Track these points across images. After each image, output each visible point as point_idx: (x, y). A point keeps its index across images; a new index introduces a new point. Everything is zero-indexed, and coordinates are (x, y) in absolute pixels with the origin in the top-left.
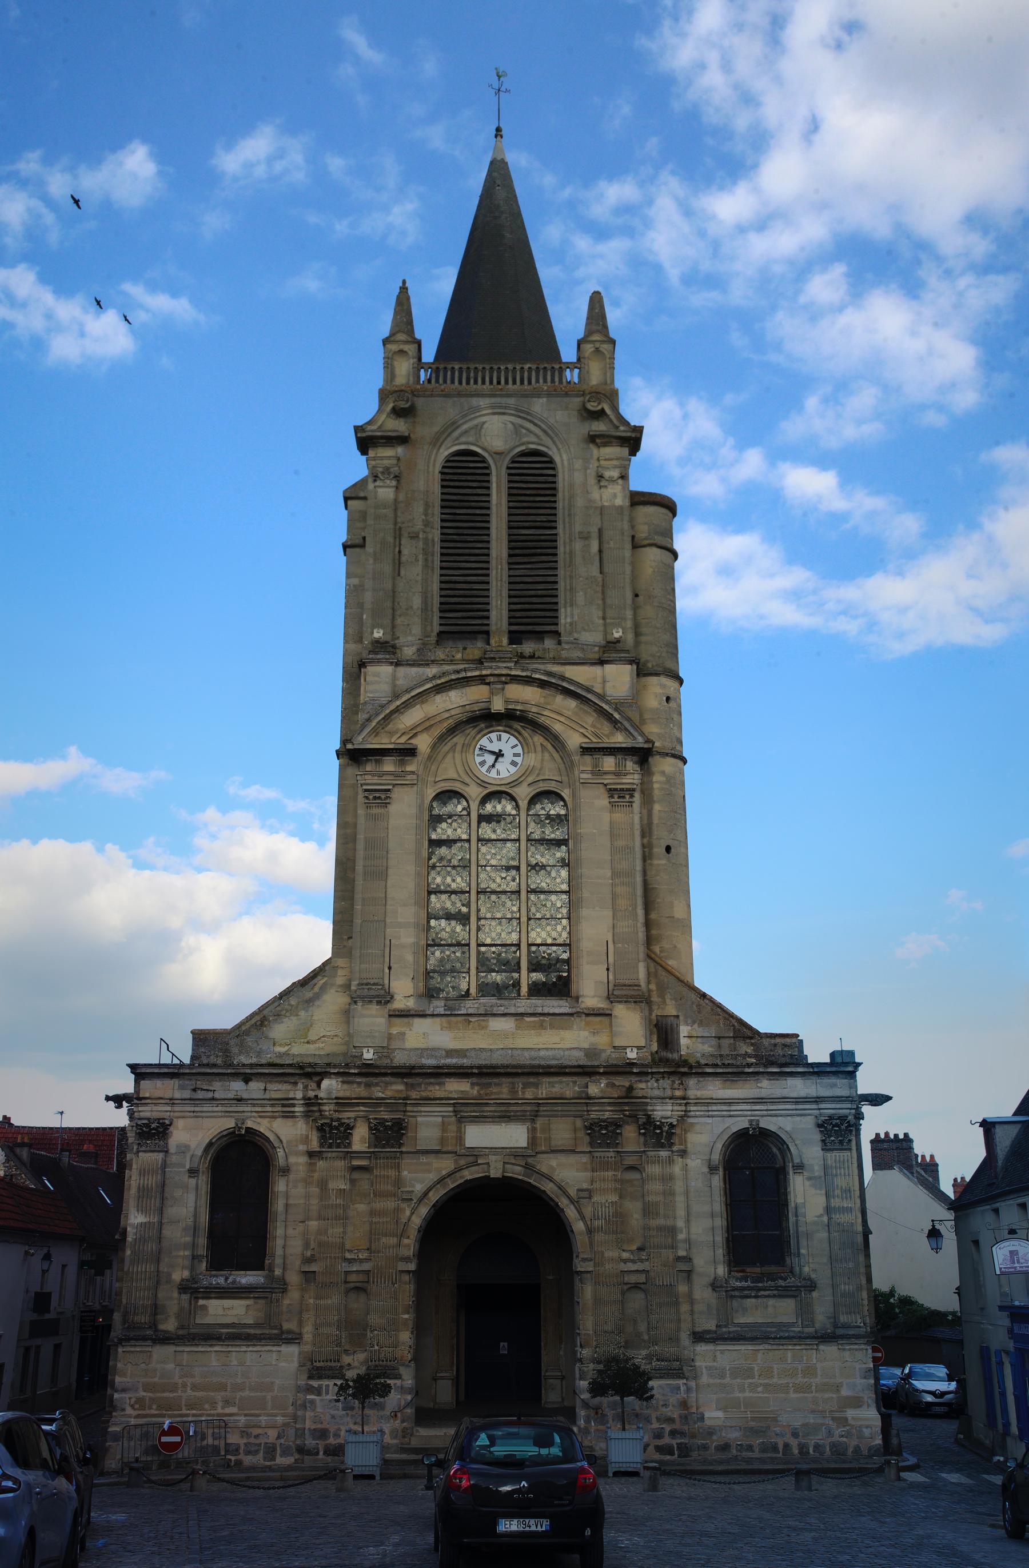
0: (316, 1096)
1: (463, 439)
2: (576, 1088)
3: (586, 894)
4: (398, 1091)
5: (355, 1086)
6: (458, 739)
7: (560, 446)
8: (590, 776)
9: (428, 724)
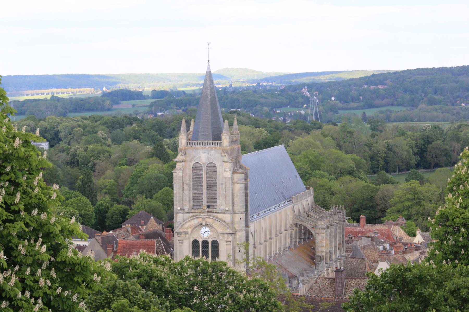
6: (197, 228)
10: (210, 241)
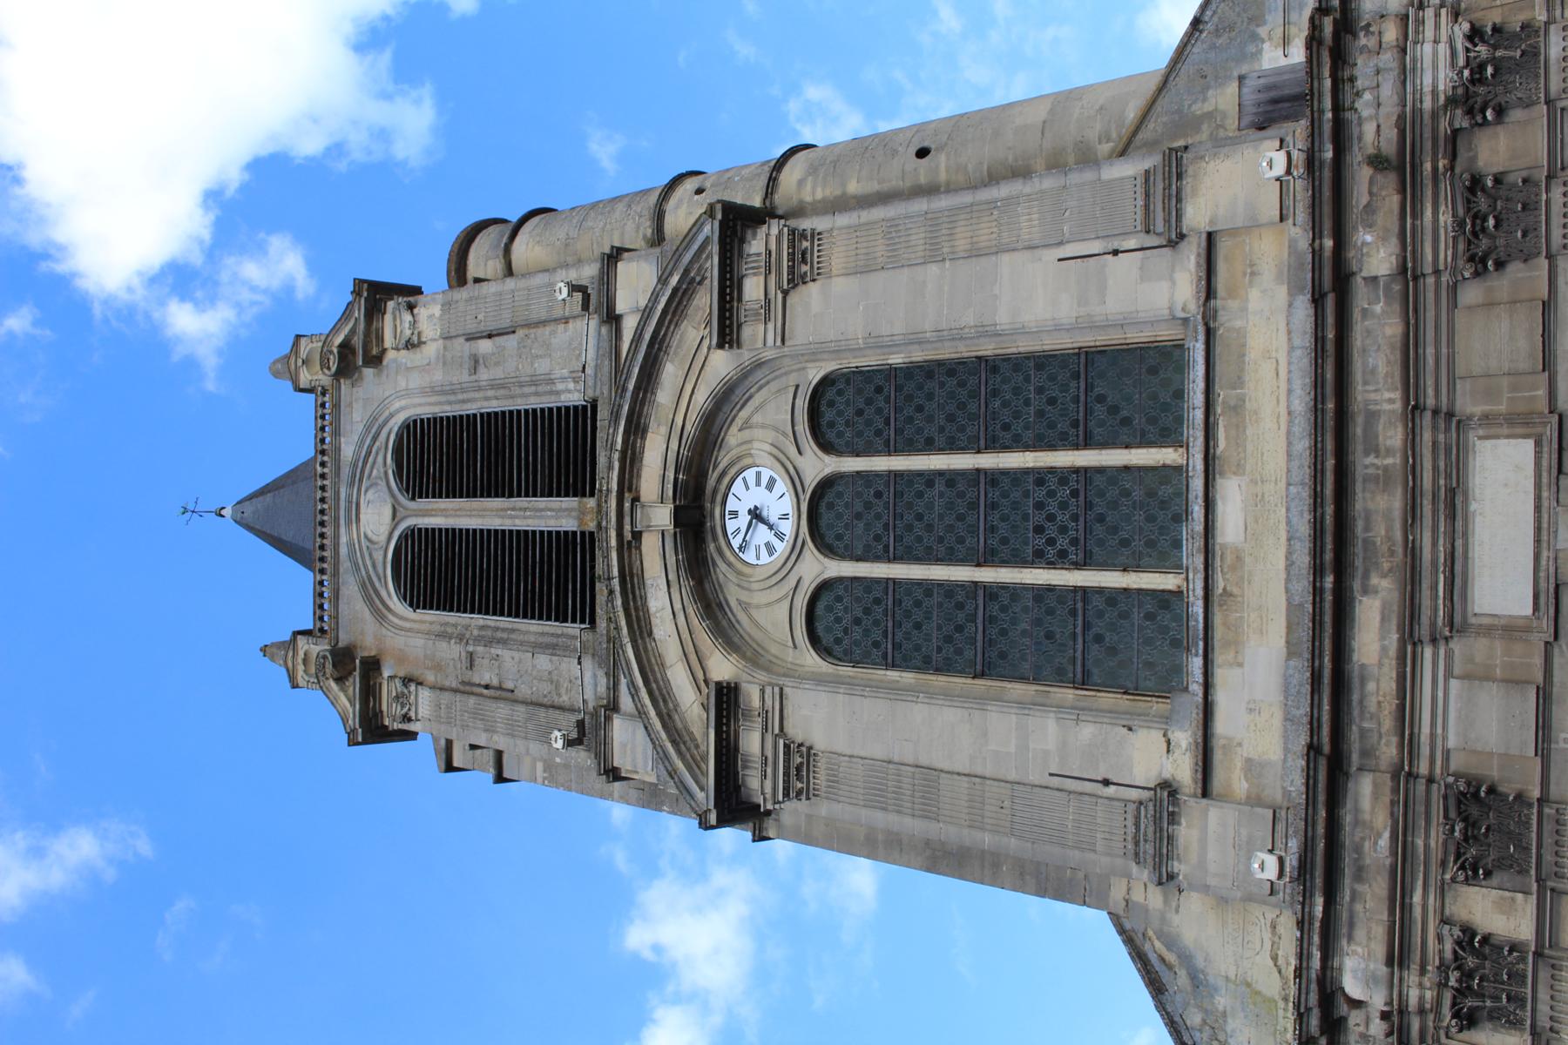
0: (1385, 1016)
1: (380, 571)
2: (1378, 308)
3: (969, 319)
4: (1376, 796)
5: (1359, 907)
7: (387, 413)
8: (771, 326)
9: (693, 657)
10: (817, 465)
